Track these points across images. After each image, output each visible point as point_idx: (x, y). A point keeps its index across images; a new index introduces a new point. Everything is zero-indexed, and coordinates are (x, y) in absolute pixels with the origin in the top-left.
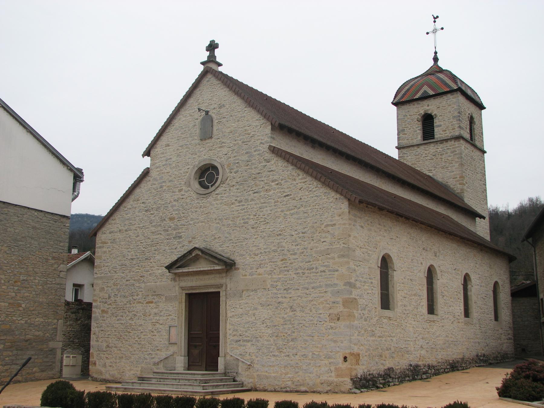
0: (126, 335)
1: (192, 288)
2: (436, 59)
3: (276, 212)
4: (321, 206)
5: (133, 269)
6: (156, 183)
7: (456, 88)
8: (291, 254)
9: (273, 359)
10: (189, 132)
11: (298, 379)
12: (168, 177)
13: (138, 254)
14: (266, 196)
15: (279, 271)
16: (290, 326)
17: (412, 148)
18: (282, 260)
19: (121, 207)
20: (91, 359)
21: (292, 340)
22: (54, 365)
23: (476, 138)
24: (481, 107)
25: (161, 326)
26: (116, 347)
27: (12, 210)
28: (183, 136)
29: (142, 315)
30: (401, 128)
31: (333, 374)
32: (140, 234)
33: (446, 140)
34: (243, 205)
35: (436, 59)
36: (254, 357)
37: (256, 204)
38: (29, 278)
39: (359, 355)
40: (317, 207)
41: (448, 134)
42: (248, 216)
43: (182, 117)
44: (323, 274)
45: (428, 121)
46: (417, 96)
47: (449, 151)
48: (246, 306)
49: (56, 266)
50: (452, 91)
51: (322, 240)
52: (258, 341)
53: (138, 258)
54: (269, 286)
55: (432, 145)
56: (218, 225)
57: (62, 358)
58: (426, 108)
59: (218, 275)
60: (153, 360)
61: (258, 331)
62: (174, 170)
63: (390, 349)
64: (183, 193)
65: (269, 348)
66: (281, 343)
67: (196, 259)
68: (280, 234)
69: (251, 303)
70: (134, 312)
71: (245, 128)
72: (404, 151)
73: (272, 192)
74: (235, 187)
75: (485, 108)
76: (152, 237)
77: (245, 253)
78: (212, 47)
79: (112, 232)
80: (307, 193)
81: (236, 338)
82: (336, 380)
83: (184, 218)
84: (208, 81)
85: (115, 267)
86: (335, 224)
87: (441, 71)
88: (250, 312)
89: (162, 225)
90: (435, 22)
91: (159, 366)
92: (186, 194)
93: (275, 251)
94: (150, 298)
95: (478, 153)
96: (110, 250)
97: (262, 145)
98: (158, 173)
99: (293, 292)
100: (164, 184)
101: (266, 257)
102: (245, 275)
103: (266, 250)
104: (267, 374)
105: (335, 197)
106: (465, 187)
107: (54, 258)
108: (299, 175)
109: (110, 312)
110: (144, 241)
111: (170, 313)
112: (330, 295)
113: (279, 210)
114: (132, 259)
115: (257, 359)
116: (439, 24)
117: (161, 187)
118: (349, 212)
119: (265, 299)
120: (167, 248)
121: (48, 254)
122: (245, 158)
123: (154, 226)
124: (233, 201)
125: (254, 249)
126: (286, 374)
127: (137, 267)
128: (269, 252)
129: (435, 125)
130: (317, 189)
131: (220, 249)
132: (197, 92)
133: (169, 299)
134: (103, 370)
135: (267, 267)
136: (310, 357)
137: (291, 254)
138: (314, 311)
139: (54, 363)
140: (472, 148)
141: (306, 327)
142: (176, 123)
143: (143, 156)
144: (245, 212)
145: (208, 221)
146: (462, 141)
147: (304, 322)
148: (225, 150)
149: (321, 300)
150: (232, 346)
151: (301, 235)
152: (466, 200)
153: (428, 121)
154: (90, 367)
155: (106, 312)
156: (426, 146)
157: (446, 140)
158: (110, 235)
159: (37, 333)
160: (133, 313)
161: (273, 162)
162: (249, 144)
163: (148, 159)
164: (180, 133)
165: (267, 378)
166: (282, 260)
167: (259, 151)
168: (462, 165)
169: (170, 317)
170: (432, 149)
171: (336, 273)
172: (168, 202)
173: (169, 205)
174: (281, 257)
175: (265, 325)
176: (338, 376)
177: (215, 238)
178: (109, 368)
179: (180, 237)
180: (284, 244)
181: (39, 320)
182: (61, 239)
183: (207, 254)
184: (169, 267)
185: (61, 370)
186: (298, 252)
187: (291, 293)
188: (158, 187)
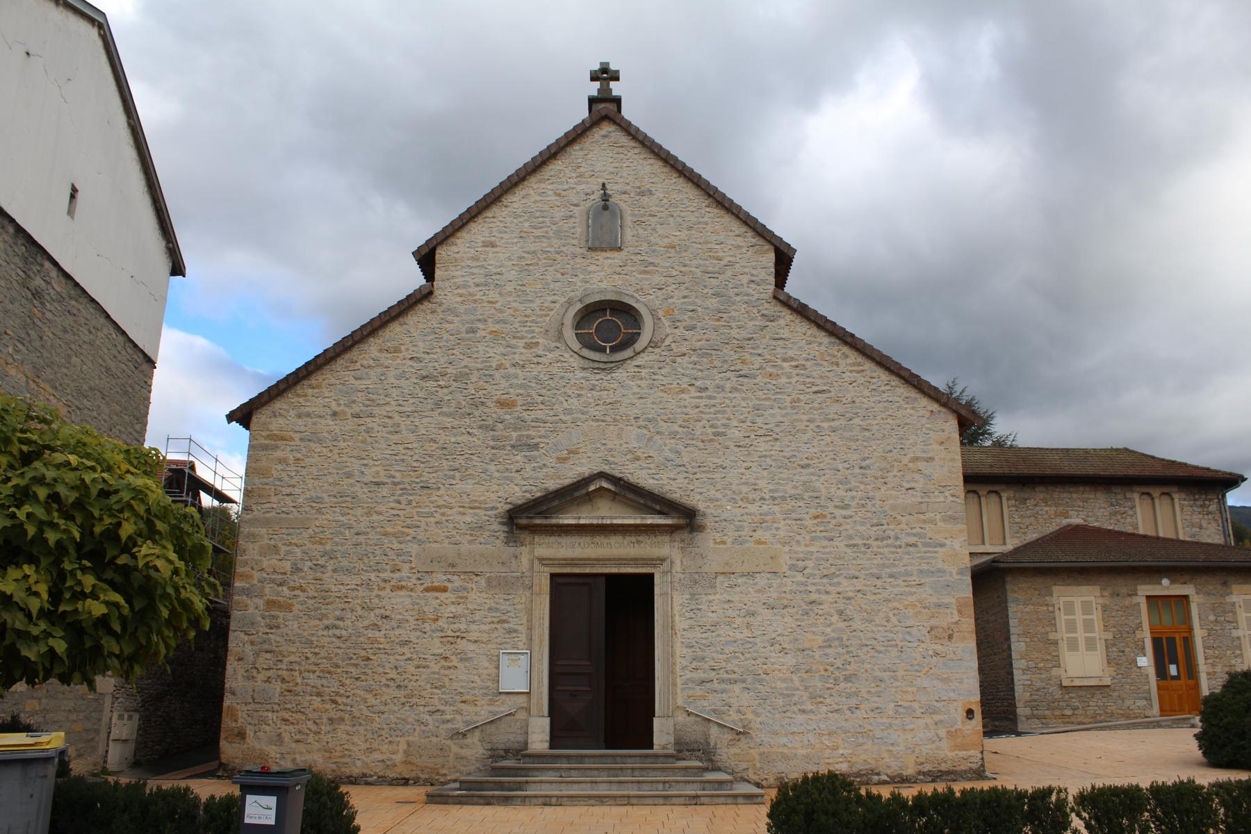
0: (356, 665)
1: (572, 562)
3: (797, 420)
4: (899, 422)
5: (382, 508)
6: (456, 319)
8: (836, 507)
9: (801, 718)
10: (554, 227)
11: (864, 757)
12: (493, 311)
13: (397, 475)
14: (770, 386)
15: (808, 537)
16: (840, 650)
18: (816, 517)
19: (340, 361)
20: (227, 723)
21: (847, 679)
25: (472, 647)
26: (319, 694)
27: (87, 312)
28: (538, 233)
29: (411, 619)
31: (944, 744)
32: (403, 427)
34: (710, 398)
36: (750, 716)
37: (743, 399)
42: (725, 421)
43: (531, 192)
48: (726, 606)
52: (760, 681)
53: (395, 484)
54: (785, 568)
56: (645, 431)
59: (666, 538)
60: (449, 726)
61: (760, 661)
62: (511, 299)
64: (540, 352)
65: (788, 696)
66: (819, 685)
67: (590, 498)
68: (808, 466)
69: (740, 602)
70: (382, 611)
71: (709, 246)
73: (784, 380)
74: (686, 358)
76: (443, 438)
77: (719, 495)
79: (308, 415)
80: (867, 393)
81: (701, 675)
82: (951, 755)
83: (541, 406)
84: (605, 136)
85: (318, 500)
86: (931, 459)
88: (739, 621)
89: (477, 413)
91: (468, 741)
92: (550, 356)
94: (439, 579)
96: (299, 456)
97: (753, 286)
98: (460, 299)
99: (845, 582)
100: (480, 325)
101: (776, 509)
102: (723, 543)
103: (776, 495)
104: (785, 750)
105: (930, 408)
108: (847, 357)
109: (297, 607)
110: (415, 445)
111: (504, 617)
112: (930, 591)
113: (804, 417)
114: (377, 484)
115: (759, 720)
117: (473, 331)
119: (775, 595)
120: (492, 468)
122: (714, 303)
123: (447, 415)
124: (684, 386)
125: (745, 489)
126: (836, 748)
127: (393, 505)
128: (784, 498)
130: (888, 387)
131: (651, 481)
133: (499, 584)
134: (273, 751)
135: (777, 529)
136: (891, 713)
137: (836, 507)
138: (894, 619)
141: (880, 652)
142: (515, 200)
144: (719, 412)
145: (615, 420)
147: (874, 642)
148: (657, 279)
149: (910, 599)
150: (691, 693)
151: (857, 471)
154: (223, 743)
155: (289, 608)
158: (300, 422)
160: (377, 611)
161: (782, 322)
162: (721, 277)
164: (527, 224)
165: (786, 758)
166: (816, 517)
167: (748, 295)
169: (506, 625)
172: (494, 365)
173: (497, 375)
174: (813, 511)
175: (777, 647)
176: (957, 747)
177: (638, 459)
178: (294, 745)
179: (536, 447)
180: (818, 484)
183: (627, 492)
186: (853, 504)
187: (839, 583)
188: (464, 329)
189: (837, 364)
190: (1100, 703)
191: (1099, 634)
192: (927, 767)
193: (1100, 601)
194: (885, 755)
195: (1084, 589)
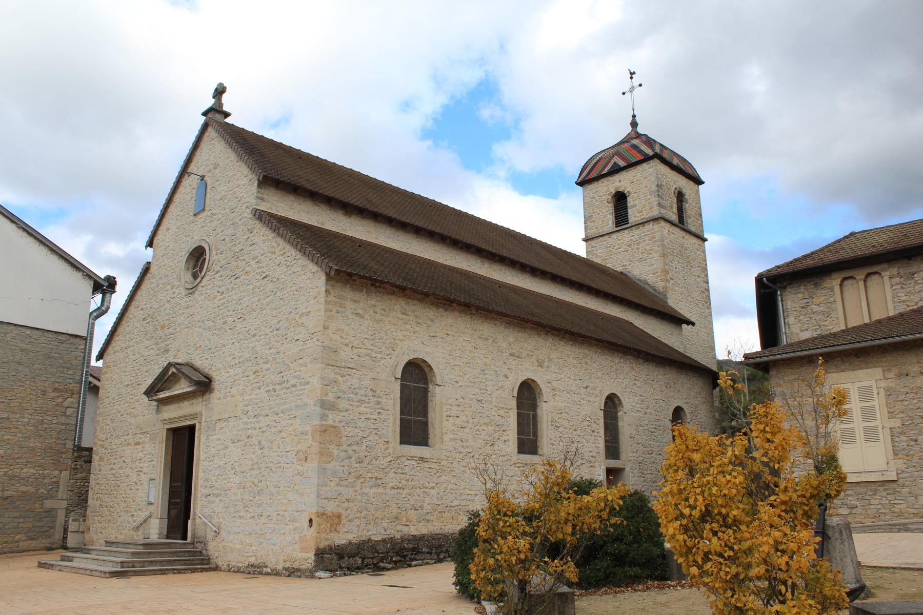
1: (171, 420)
2: (634, 124)
7: (651, 153)
17: (601, 239)
22: (52, 531)
23: (689, 221)
24: (699, 182)
30: (588, 215)
31: (297, 546)
33: (643, 224)
35: (634, 124)
36: (221, 520)
38: (14, 416)
39: (339, 516)
40: (294, 288)
41: (646, 215)
44: (294, 389)
45: (620, 199)
46: (605, 171)
47: (647, 238)
49: (60, 400)
50: (647, 159)
51: (296, 338)
55: (626, 232)
57: (66, 522)
58: (617, 184)
63: (422, 507)
72: (593, 243)
75: (703, 183)
78: (220, 92)
82: (299, 555)
86: (310, 312)
87: (638, 136)
90: (631, 78)
93: (248, 360)
95: (695, 240)
106: (670, 285)
107: (55, 389)
108: (279, 245)
114: (128, 385)
116: (637, 80)
118: (327, 291)
121: (46, 385)
129: (629, 205)
132: (198, 153)
139: (53, 528)
140: (683, 233)
143: (146, 247)
146: (663, 223)
149: (291, 429)
151: (275, 332)
152: (671, 302)
153: (620, 199)
156: (618, 234)
157: (643, 224)
159: (24, 489)
163: (150, 250)
166: (255, 373)
168: (664, 255)
170: (626, 236)
171: (307, 387)
174: (254, 369)
181: (28, 471)
182: (69, 366)
184: (150, 392)
185: (65, 538)
189: (274, 252)
190: (884, 501)
191: (882, 422)
192: (288, 565)
193: (883, 384)
194: (270, 553)
195: (861, 373)
